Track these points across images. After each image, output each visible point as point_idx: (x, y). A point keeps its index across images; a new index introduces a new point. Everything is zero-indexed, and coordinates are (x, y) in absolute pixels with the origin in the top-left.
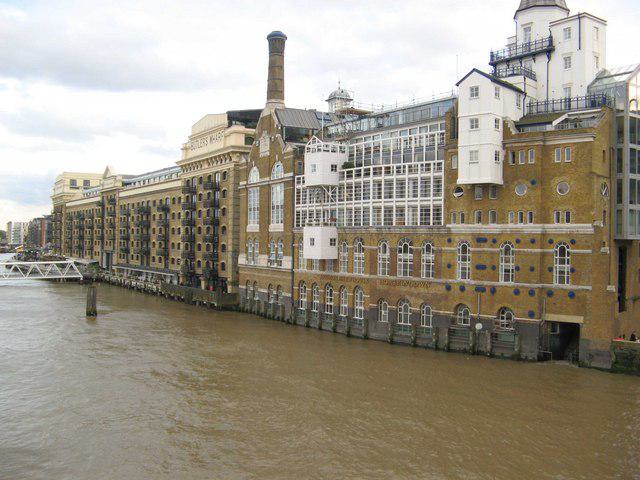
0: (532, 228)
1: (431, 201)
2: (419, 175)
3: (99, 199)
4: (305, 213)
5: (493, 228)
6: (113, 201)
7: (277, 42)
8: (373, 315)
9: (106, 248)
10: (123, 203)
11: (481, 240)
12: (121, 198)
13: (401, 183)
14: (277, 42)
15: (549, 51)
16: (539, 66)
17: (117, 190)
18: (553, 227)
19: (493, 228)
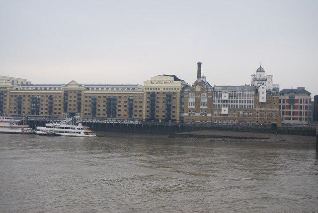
0: (269, 109)
1: (252, 104)
2: (249, 100)
3: (61, 92)
4: (216, 105)
5: (264, 109)
6: (80, 95)
7: (199, 65)
8: (238, 124)
9: (68, 111)
10: (87, 95)
11: (261, 111)
12: (85, 93)
13: (237, 101)
14: (199, 65)
15: (266, 80)
16: (264, 82)
17: (80, 91)
18: (272, 109)
19: (264, 109)
